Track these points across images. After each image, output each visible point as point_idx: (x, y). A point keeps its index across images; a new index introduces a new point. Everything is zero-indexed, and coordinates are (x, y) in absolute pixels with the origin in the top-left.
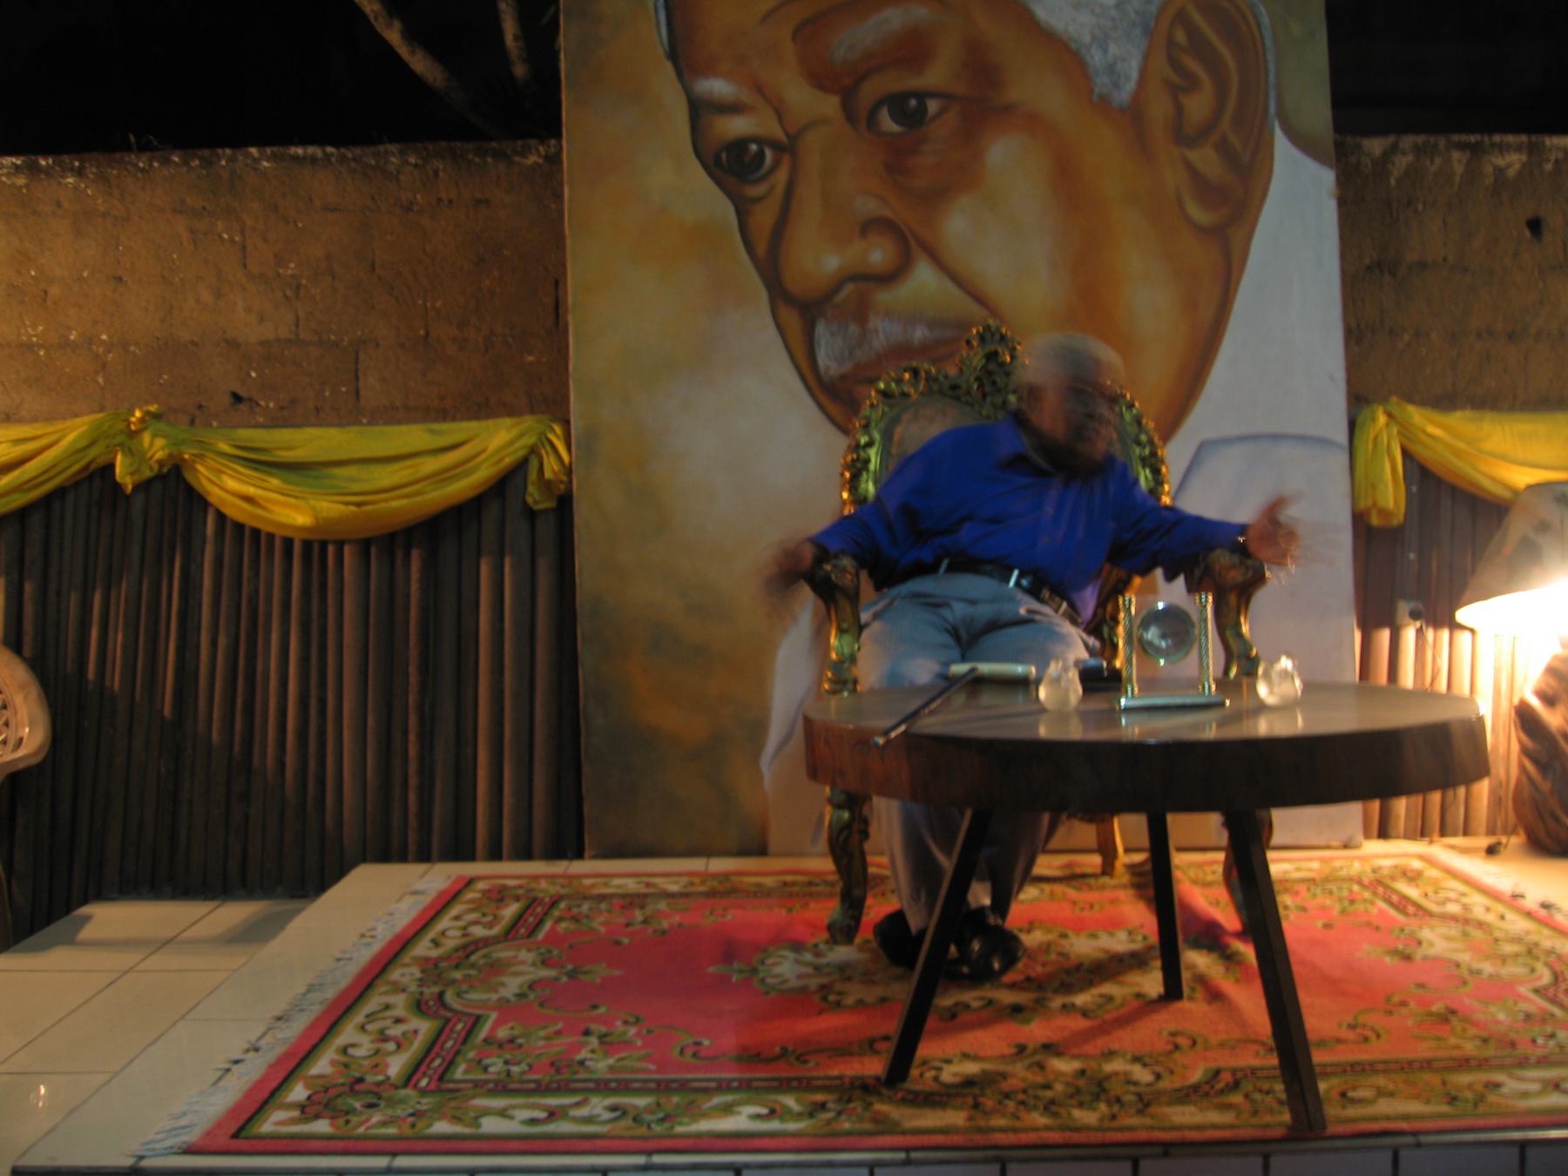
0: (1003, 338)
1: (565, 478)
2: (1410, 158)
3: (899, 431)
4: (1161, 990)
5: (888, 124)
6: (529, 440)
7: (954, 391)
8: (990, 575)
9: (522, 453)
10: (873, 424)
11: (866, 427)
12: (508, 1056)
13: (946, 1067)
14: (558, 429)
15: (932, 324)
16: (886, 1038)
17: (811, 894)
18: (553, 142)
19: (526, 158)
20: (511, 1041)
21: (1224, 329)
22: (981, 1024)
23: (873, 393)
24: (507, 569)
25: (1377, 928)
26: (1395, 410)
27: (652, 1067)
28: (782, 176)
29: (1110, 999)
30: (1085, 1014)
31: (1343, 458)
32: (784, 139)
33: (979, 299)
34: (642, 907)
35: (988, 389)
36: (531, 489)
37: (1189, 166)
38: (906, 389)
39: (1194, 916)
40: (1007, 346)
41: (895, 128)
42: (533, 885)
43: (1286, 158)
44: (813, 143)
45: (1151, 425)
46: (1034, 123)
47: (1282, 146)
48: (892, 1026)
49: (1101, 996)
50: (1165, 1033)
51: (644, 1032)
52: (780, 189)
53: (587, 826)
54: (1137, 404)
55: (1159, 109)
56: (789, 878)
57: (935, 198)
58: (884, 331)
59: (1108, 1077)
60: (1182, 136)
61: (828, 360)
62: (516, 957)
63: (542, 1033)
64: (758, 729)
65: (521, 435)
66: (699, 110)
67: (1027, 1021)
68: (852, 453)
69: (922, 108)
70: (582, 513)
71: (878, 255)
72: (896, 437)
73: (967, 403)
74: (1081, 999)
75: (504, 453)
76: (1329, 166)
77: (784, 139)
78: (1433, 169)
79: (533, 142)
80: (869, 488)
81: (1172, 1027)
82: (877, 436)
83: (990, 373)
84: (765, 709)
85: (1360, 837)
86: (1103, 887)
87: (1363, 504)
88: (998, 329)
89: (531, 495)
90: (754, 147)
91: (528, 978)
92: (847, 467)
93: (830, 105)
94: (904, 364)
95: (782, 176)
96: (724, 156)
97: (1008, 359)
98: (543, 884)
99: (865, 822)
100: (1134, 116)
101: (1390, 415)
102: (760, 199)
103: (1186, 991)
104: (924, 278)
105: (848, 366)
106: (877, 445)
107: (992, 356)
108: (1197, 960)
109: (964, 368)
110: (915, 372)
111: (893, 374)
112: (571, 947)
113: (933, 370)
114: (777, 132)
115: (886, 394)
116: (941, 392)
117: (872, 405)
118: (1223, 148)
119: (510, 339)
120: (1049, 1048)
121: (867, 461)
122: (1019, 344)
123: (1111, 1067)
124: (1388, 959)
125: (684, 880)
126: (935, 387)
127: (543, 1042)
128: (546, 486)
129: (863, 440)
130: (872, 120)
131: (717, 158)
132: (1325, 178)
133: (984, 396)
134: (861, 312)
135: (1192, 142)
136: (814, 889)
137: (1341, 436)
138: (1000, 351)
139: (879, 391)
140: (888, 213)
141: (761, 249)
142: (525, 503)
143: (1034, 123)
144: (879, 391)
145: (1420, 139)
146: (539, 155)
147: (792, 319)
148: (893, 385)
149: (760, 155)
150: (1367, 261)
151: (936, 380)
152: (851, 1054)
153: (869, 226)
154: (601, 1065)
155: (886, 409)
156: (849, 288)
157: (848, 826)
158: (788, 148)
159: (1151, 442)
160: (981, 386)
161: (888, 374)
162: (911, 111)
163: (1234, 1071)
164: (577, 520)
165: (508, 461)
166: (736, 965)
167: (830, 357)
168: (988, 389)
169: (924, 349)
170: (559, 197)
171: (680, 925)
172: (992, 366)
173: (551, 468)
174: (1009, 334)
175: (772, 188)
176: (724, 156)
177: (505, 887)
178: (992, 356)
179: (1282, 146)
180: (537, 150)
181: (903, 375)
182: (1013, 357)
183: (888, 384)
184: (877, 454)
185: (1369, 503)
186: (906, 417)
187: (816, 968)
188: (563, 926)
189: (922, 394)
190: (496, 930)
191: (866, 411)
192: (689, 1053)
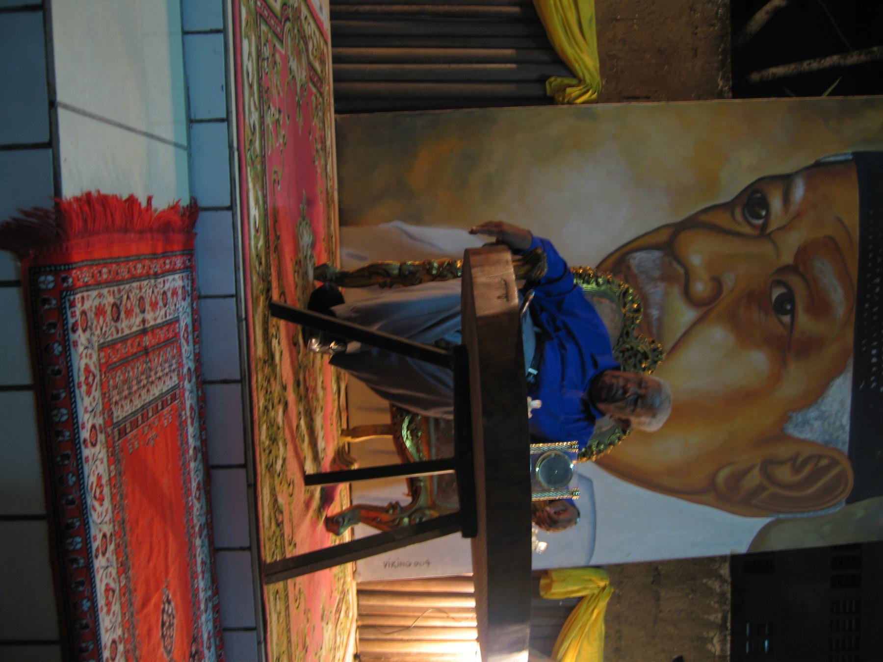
0: (655, 362)
1: (566, 101)
2: (718, 590)
3: (606, 302)
4: (307, 473)
5: (777, 292)
6: (588, 78)
8: (534, 358)
9: (581, 75)
10: (609, 286)
11: (608, 282)
12: (270, 59)
13: (277, 340)
14: (595, 96)
15: (660, 320)
16: (285, 302)
17: (329, 253)
18: (730, 95)
19: (721, 80)
20: (275, 63)
22: (292, 362)
23: (626, 286)
24: (509, 66)
25: (331, 597)
26: (607, 590)
27: (270, 152)
28: (747, 230)
29: (303, 441)
30: (298, 426)
31: (583, 563)
32: (768, 231)
34: (322, 149)
35: (627, 354)
36: (559, 80)
39: (333, 489)
41: (774, 297)
42: (326, 84)
44: (767, 248)
45: (609, 450)
46: (776, 378)
47: (760, 522)
48: (289, 304)
49: (304, 436)
50: (293, 477)
51: (281, 148)
52: (740, 229)
53: (354, 116)
54: (620, 442)
55: (783, 451)
56: (334, 238)
57: (733, 320)
58: (656, 291)
59: (277, 444)
60: (768, 464)
61: (639, 259)
62: (303, 69)
63: (278, 83)
64: (417, 219)
65: (590, 74)
66: (786, 181)
67: (294, 391)
69: (785, 313)
70: (546, 111)
71: (700, 288)
74: (302, 422)
75: (581, 63)
76: (748, 550)
77: (768, 231)
78: (712, 603)
79: (731, 83)
81: (296, 481)
82: (603, 288)
83: (636, 355)
84: (431, 223)
85: (360, 580)
86: (338, 430)
87: (554, 576)
88: (659, 360)
89: (555, 80)
91: (296, 76)
92: (585, 270)
93: (788, 259)
94: (642, 304)
95: (747, 230)
96: (759, 195)
97: (643, 366)
98: (327, 88)
99: (391, 286)
100: (779, 436)
101: (604, 588)
103: (308, 487)
104: (687, 315)
105: (635, 270)
106: (598, 288)
107: (645, 356)
108: (317, 489)
110: (637, 311)
111: (637, 297)
112: (308, 104)
113: (638, 321)
114: (772, 227)
115: (625, 293)
116: (625, 326)
118: (761, 488)
119: (615, 70)
120: (286, 405)
121: (588, 283)
122: (652, 372)
123: (281, 444)
124: (321, 606)
125: (331, 176)
126: (628, 323)
127: (275, 81)
128: (562, 89)
129: (600, 280)
130: (779, 283)
132: (742, 548)
133: (623, 352)
134: (667, 278)
136: (331, 254)
137: (594, 561)
138: (648, 361)
140: (724, 293)
141: (705, 218)
142: (550, 76)
143: (776, 378)
145: (729, 595)
146: (722, 87)
147: (663, 237)
148: (631, 298)
149: (759, 217)
150: (660, 568)
151: (633, 323)
152: (279, 280)
153: (717, 282)
154: (269, 120)
155: (617, 294)
156: (681, 271)
158: (763, 233)
159: (599, 452)
160: (628, 350)
162: (784, 305)
163: (282, 522)
164: (542, 108)
165: (577, 66)
166: (305, 207)
167: (640, 259)
169: (647, 316)
170: (699, 98)
171: (317, 173)
172: (639, 356)
173: (573, 92)
176: (759, 195)
177: (325, 64)
178: (645, 356)
179: (760, 522)
180: (726, 86)
181: (636, 304)
182: (644, 369)
183: (631, 294)
184: (592, 288)
185: (554, 578)
186: (614, 306)
187: (306, 257)
188: (313, 98)
189: (625, 315)
190: (311, 57)
191: (617, 281)
192: (274, 176)
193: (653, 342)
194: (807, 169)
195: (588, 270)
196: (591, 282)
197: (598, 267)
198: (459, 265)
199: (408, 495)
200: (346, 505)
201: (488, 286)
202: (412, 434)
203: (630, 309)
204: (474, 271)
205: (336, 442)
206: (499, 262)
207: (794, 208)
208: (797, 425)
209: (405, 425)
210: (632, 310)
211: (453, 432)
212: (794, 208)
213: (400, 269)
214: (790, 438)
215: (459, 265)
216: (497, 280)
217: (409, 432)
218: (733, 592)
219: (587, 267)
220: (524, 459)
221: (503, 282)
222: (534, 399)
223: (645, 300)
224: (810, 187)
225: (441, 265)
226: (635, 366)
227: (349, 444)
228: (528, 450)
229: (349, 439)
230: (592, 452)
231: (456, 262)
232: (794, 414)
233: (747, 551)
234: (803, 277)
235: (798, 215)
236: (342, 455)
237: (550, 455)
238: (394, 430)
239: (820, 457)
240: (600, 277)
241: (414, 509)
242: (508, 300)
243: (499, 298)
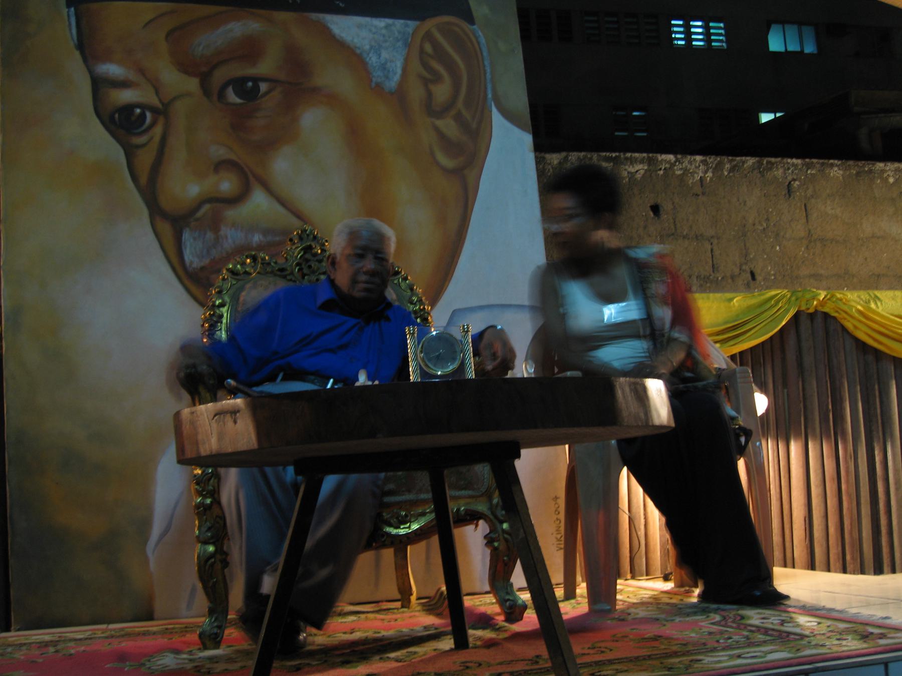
0: (315, 238)
5: (233, 97)
7: (282, 272)
11: (220, 292)
15: (266, 232)
21: (465, 239)
28: (158, 130)
32: (160, 106)
33: (298, 215)
37: (437, 129)
38: (247, 270)
39: (472, 612)
40: (318, 242)
41: (238, 101)
43: (501, 128)
44: (180, 108)
46: (332, 100)
47: (497, 117)
52: (157, 139)
54: (409, 278)
55: (416, 93)
58: (231, 237)
60: (432, 110)
61: (192, 256)
64: (145, 525)
66: (99, 85)
68: (209, 310)
69: (256, 88)
71: (227, 185)
72: (241, 299)
73: (291, 280)
76: (528, 131)
77: (160, 106)
80: (224, 335)
82: (227, 299)
83: (307, 261)
84: (150, 509)
86: (403, 612)
90: (138, 111)
92: (206, 320)
93: (192, 84)
94: (246, 254)
95: (158, 130)
96: (117, 116)
97: (319, 251)
100: (400, 96)
102: (143, 145)
104: (259, 200)
105: (206, 261)
106: (228, 306)
109: (289, 257)
110: (254, 259)
113: (267, 258)
114: (155, 101)
115: (233, 273)
116: (272, 272)
117: (224, 279)
118: (458, 118)
121: (221, 316)
122: (327, 241)
126: (269, 269)
130: (221, 95)
131: (112, 117)
132: (527, 139)
133: (303, 276)
134: (215, 224)
135: (440, 114)
139: (228, 270)
140: (233, 157)
141: (143, 180)
143: (332, 100)
144: (228, 270)
147: (166, 229)
148: (239, 266)
149: (143, 116)
151: (269, 264)
153: (220, 166)
155: (234, 282)
156: (207, 207)
157: (212, 555)
158: (163, 112)
161: (236, 260)
167: (192, 256)
168: (305, 271)
169: (260, 248)
172: (308, 256)
174: (319, 235)
175: (151, 139)
176: (117, 116)
179: (497, 117)
181: (246, 261)
182: (323, 251)
183: (235, 266)
186: (248, 286)
191: (219, 282)
193: (291, 240)
194: (85, 60)
195: (206, 317)
196: (221, 314)
197: (202, 305)
198: (199, 471)
199: (477, 526)
200: (490, 599)
201: (221, 437)
202: (405, 523)
203: (253, 267)
204: (204, 451)
205: (417, 614)
206: (193, 423)
207: (132, 76)
208: (387, 77)
209: (394, 531)
210: (253, 264)
211: (400, 473)
212: (132, 76)
213: (206, 542)
215: (199, 471)
216: (214, 425)
217: (402, 527)
218: (581, 151)
219: (202, 319)
220: (427, 387)
221: (216, 418)
222: (357, 380)
223: (241, 250)
224: (107, 58)
225: (199, 493)
226: (320, 261)
227: (418, 599)
228: (415, 384)
229: (413, 598)
230: (421, 310)
231: (195, 476)
232: (374, 80)
233: (530, 134)
234: (214, 67)
235: (142, 71)
236: (430, 607)
237: (423, 359)
238: (400, 544)
240: (215, 302)
241: (491, 517)
242: (238, 411)
243: (235, 422)
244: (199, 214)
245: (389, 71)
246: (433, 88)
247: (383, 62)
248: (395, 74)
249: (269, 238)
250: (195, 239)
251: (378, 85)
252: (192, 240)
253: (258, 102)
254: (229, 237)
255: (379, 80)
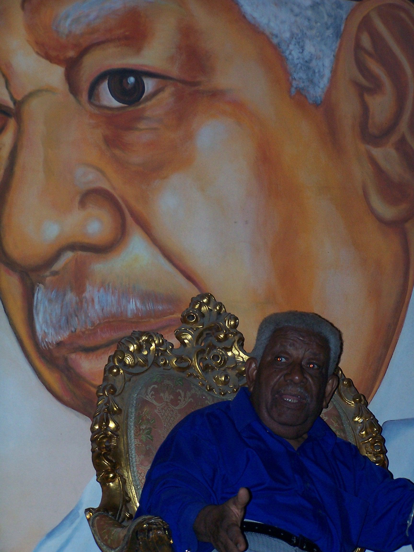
41: (115, 103)
140: (106, 186)
208: (311, 81)
214: (329, 93)
232: (294, 83)
239: (358, 46)
244: (58, 266)
245: (314, 72)
246: (368, 98)
247: (307, 58)
248: (322, 77)
249: (150, 306)
250: (50, 301)
251: (299, 91)
252: (46, 303)
253: (141, 107)
254: (96, 300)
255: (301, 85)
